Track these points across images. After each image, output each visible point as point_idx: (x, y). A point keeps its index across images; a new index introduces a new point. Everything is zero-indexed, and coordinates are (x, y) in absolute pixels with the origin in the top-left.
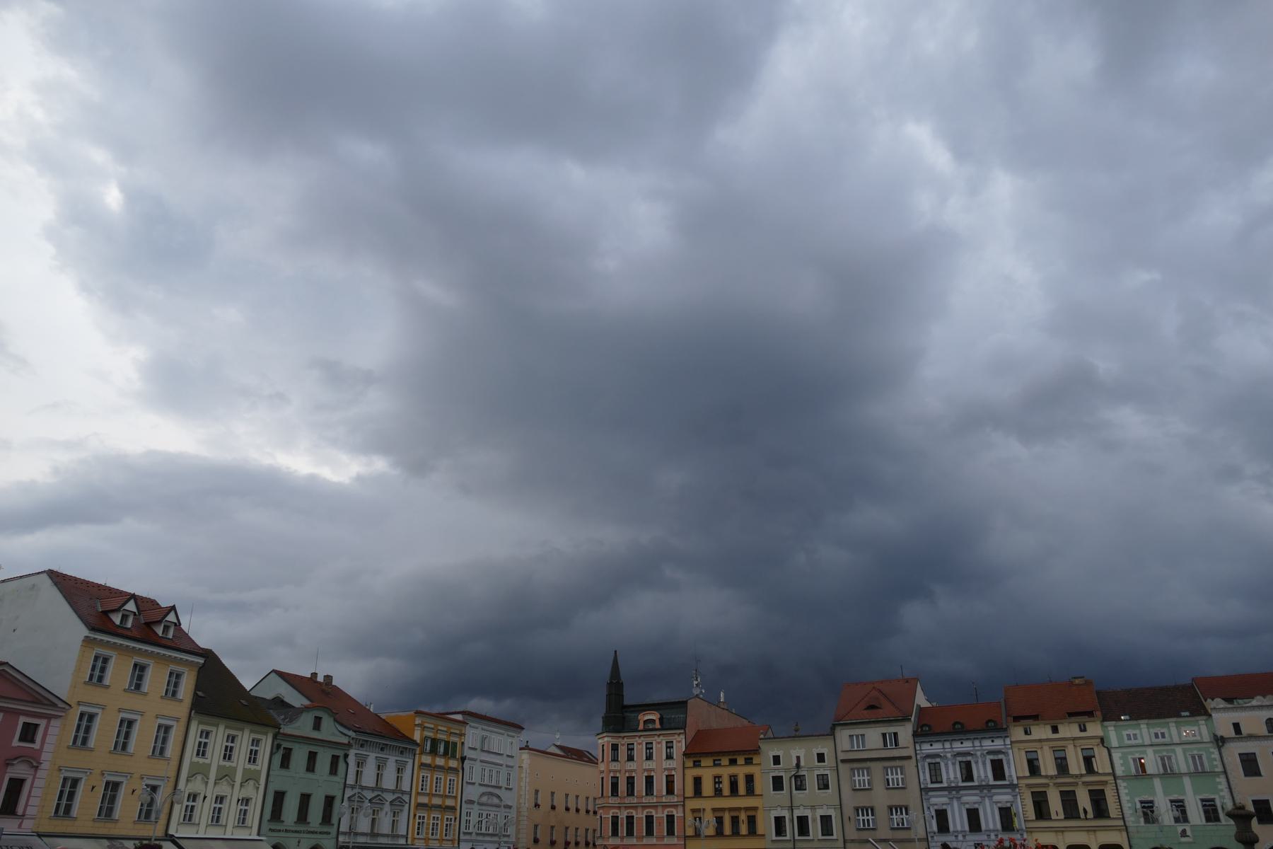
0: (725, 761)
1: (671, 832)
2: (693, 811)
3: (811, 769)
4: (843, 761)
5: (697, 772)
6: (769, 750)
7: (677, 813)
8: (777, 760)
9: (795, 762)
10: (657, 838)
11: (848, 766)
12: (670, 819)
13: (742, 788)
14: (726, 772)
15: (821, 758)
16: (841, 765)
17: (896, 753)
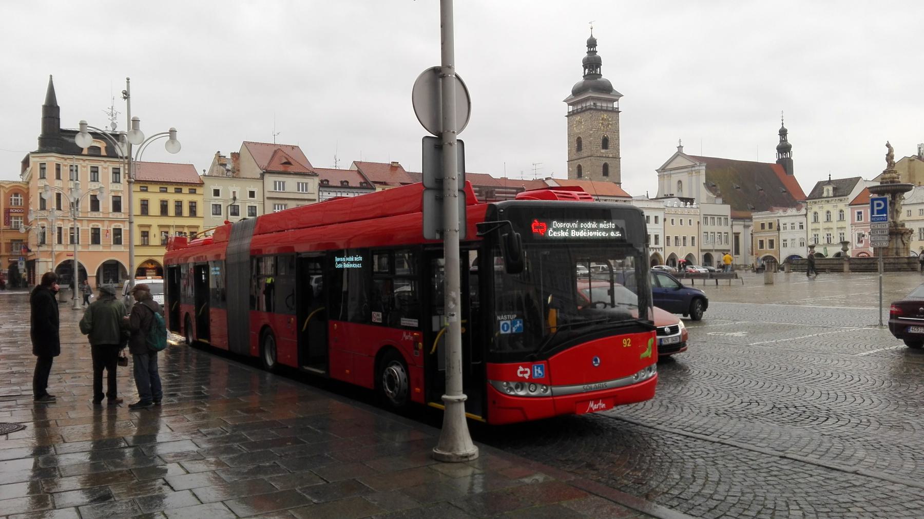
0: (171, 189)
1: (118, 241)
2: (141, 226)
3: (244, 202)
4: (269, 198)
5: (144, 196)
6: (211, 186)
7: (125, 227)
8: (217, 193)
9: (232, 197)
10: (83, 246)
11: (272, 202)
12: (118, 232)
13: (186, 210)
14: (171, 198)
15: (252, 194)
16: (267, 201)
17: (306, 197)
